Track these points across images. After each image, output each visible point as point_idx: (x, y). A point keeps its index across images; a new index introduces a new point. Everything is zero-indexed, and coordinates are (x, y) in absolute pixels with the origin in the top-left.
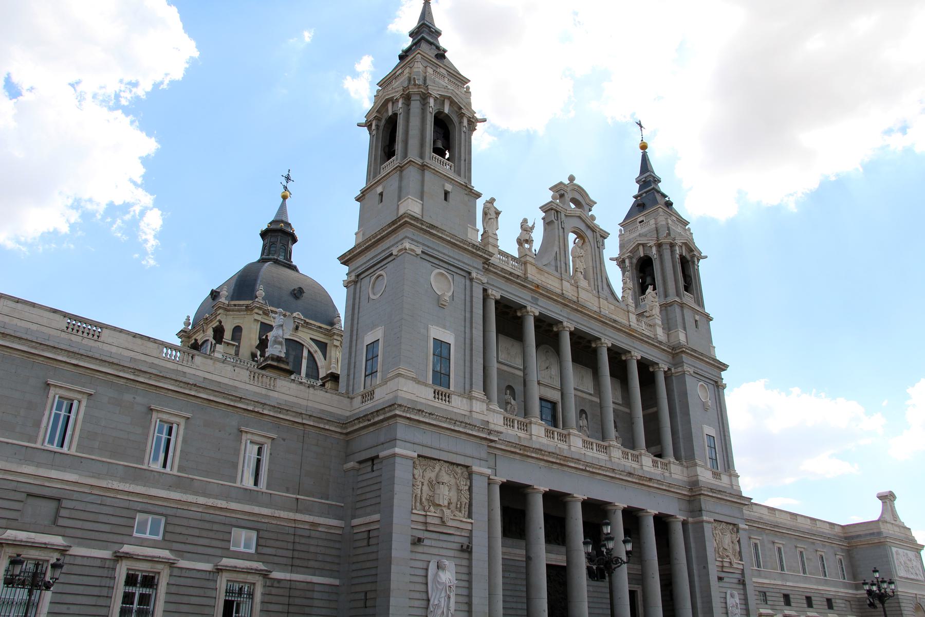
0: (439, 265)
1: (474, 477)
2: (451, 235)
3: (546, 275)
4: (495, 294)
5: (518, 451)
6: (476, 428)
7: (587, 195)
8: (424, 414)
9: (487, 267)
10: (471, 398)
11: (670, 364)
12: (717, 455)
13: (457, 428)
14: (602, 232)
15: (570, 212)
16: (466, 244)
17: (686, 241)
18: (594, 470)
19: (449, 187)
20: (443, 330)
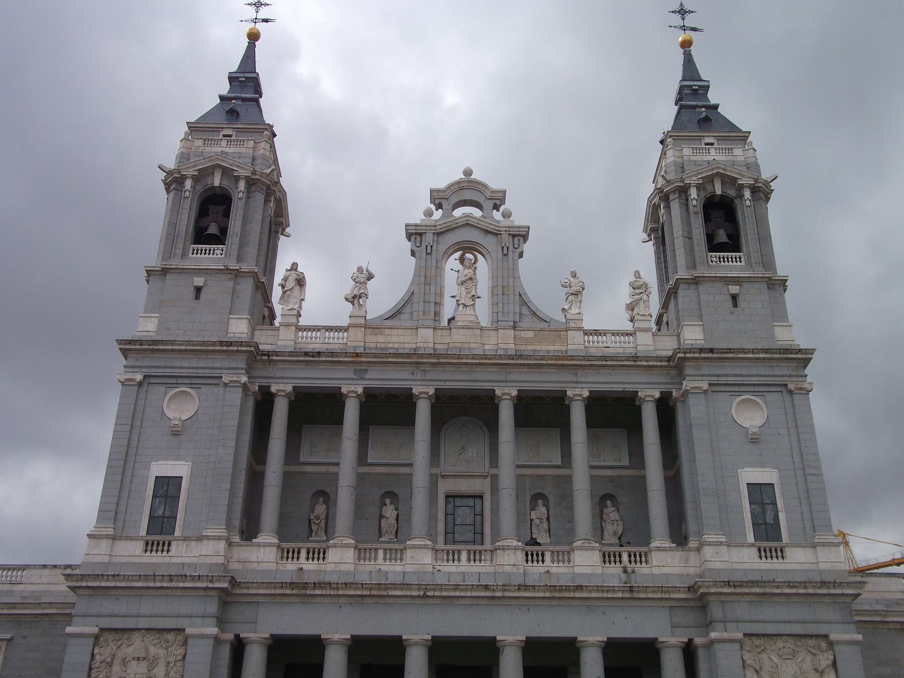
0: (177, 384)
1: (190, 642)
3: (387, 332)
4: (282, 387)
5: (288, 592)
6: (188, 578)
7: (485, 186)
8: (106, 577)
9: (266, 358)
10: (200, 538)
11: (663, 384)
12: (782, 516)
13: (158, 585)
14: (511, 229)
15: (442, 226)
16: (210, 345)
17: (717, 171)
18: (444, 594)
19: (199, 281)
20: (174, 462)
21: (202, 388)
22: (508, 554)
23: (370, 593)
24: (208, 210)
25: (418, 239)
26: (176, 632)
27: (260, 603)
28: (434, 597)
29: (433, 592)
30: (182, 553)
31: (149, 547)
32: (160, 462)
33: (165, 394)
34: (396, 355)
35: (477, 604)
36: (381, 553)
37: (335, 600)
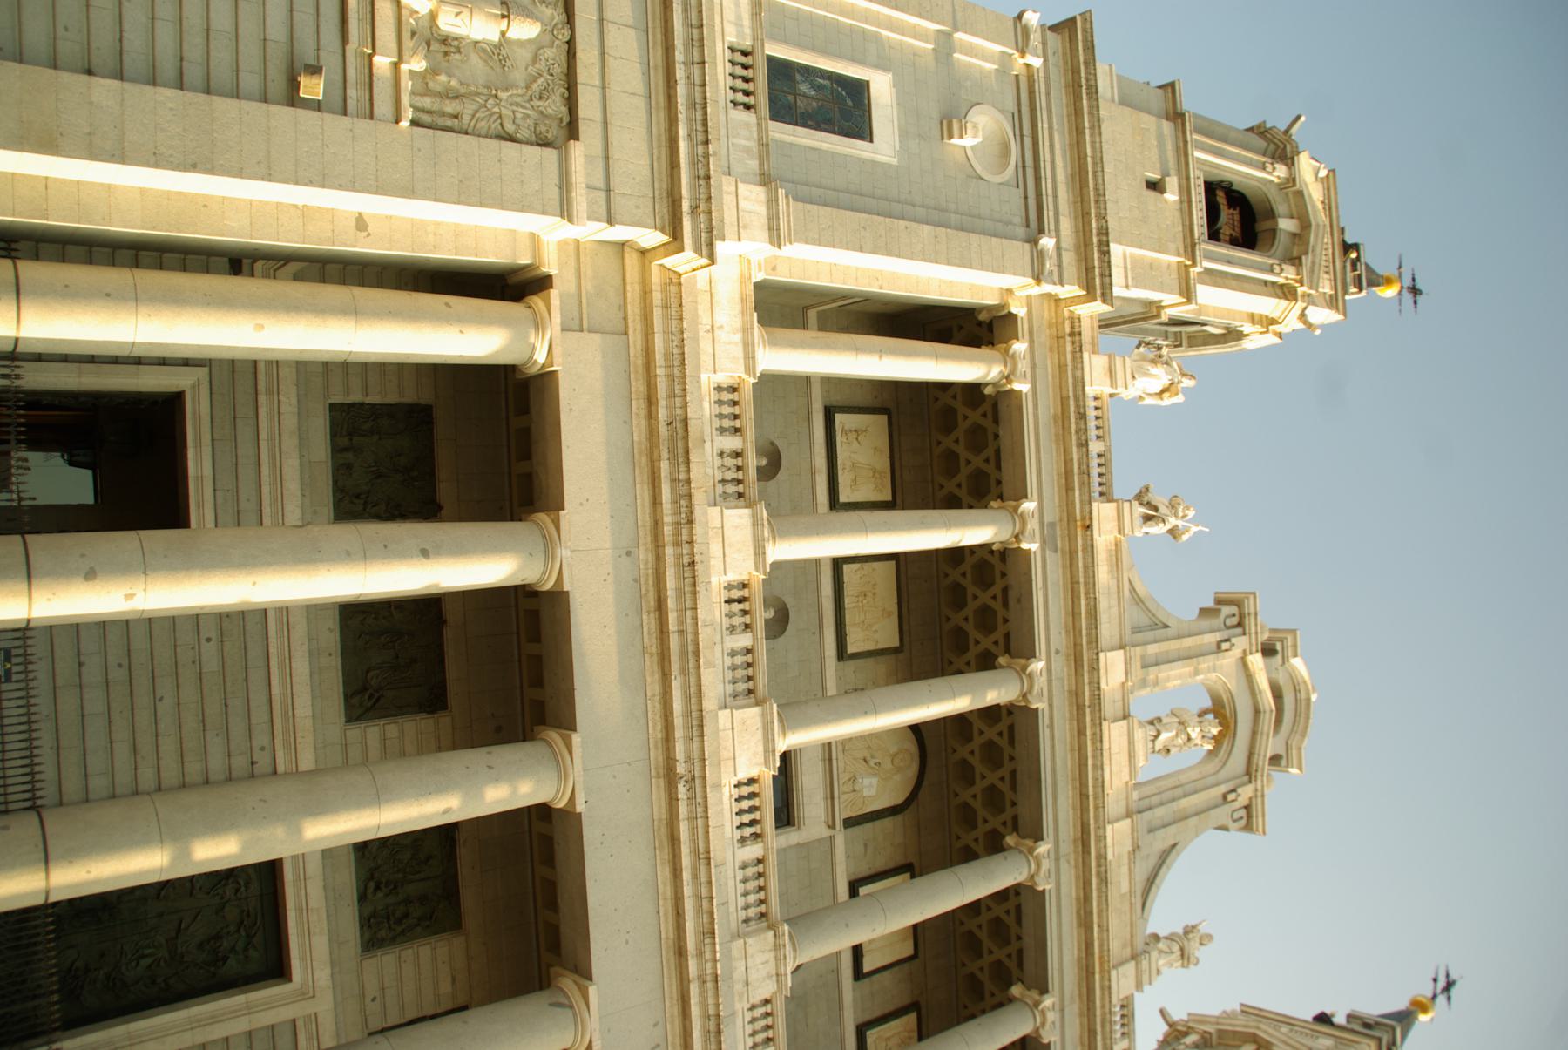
0: (1022, 136)
1: (550, 154)
2: (1099, 155)
5: (662, 414)
6: (700, 149)
7: (1303, 735)
9: (1068, 330)
13: (680, 73)
14: (1259, 800)
16: (1097, 208)
20: (896, 123)
21: (1017, 190)
22: (767, 962)
23: (673, 632)
24: (1235, 209)
25: (1235, 620)
26: (566, 119)
27: (624, 337)
28: (672, 800)
29: (685, 797)
30: (734, 137)
31: (739, 58)
32: (894, 90)
33: (1002, 111)
34: (1093, 612)
35: (658, 913)
36: (744, 640)
37: (645, 538)
